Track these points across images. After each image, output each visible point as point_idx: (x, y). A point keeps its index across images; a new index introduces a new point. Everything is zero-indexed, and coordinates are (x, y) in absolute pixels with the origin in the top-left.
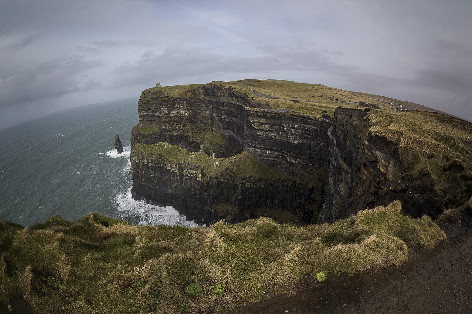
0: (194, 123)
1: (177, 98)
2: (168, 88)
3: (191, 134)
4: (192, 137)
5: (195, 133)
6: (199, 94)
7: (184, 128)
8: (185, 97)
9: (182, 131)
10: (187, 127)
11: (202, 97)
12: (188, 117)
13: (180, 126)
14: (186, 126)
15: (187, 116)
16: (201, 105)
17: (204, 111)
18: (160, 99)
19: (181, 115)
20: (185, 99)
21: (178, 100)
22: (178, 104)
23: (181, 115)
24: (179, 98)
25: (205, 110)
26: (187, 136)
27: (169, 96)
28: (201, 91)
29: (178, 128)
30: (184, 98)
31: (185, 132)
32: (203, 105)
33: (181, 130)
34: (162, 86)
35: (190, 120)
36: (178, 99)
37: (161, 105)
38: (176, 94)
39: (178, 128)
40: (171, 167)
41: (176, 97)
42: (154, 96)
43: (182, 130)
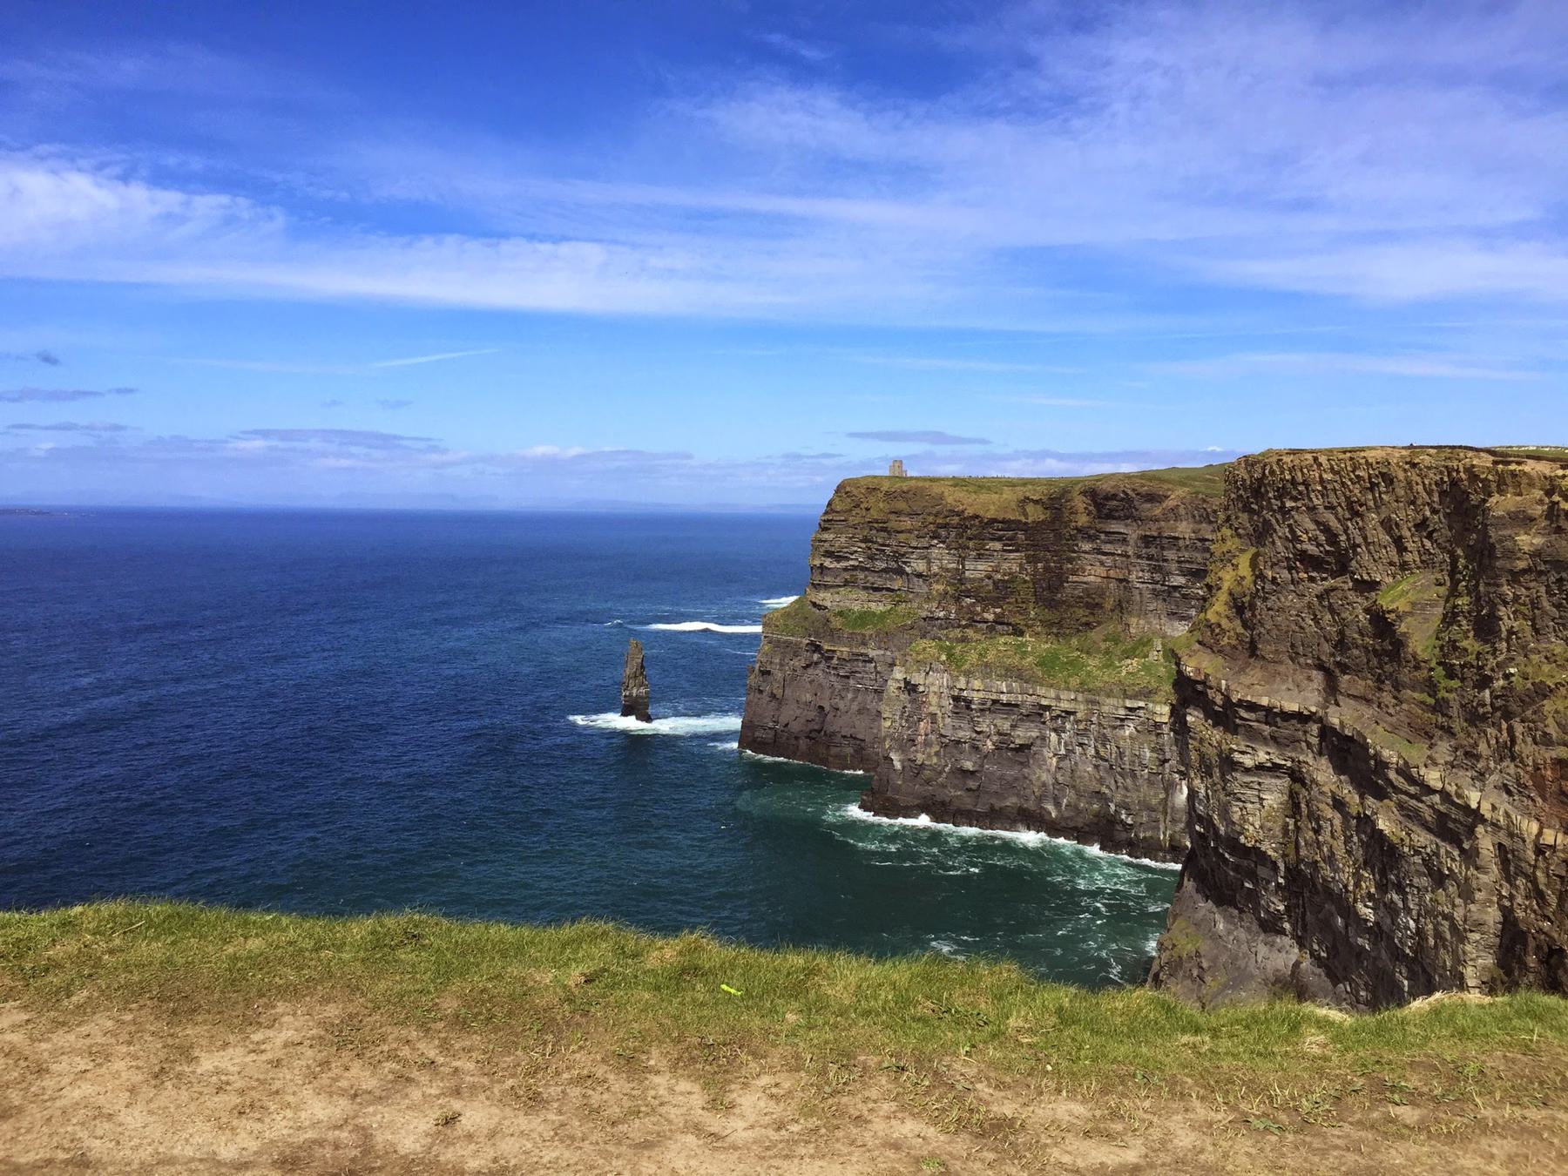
0: (1051, 604)
1: (994, 521)
5: (1057, 635)
11: (1083, 520)
14: (1024, 612)
18: (931, 519)
22: (999, 539)
28: (1080, 503)
29: (991, 617)
32: (1087, 546)
33: (1002, 623)
34: (909, 474)
37: (932, 538)
38: (989, 506)
40: (1058, 699)
41: (989, 515)
42: (901, 505)
43: (1008, 624)
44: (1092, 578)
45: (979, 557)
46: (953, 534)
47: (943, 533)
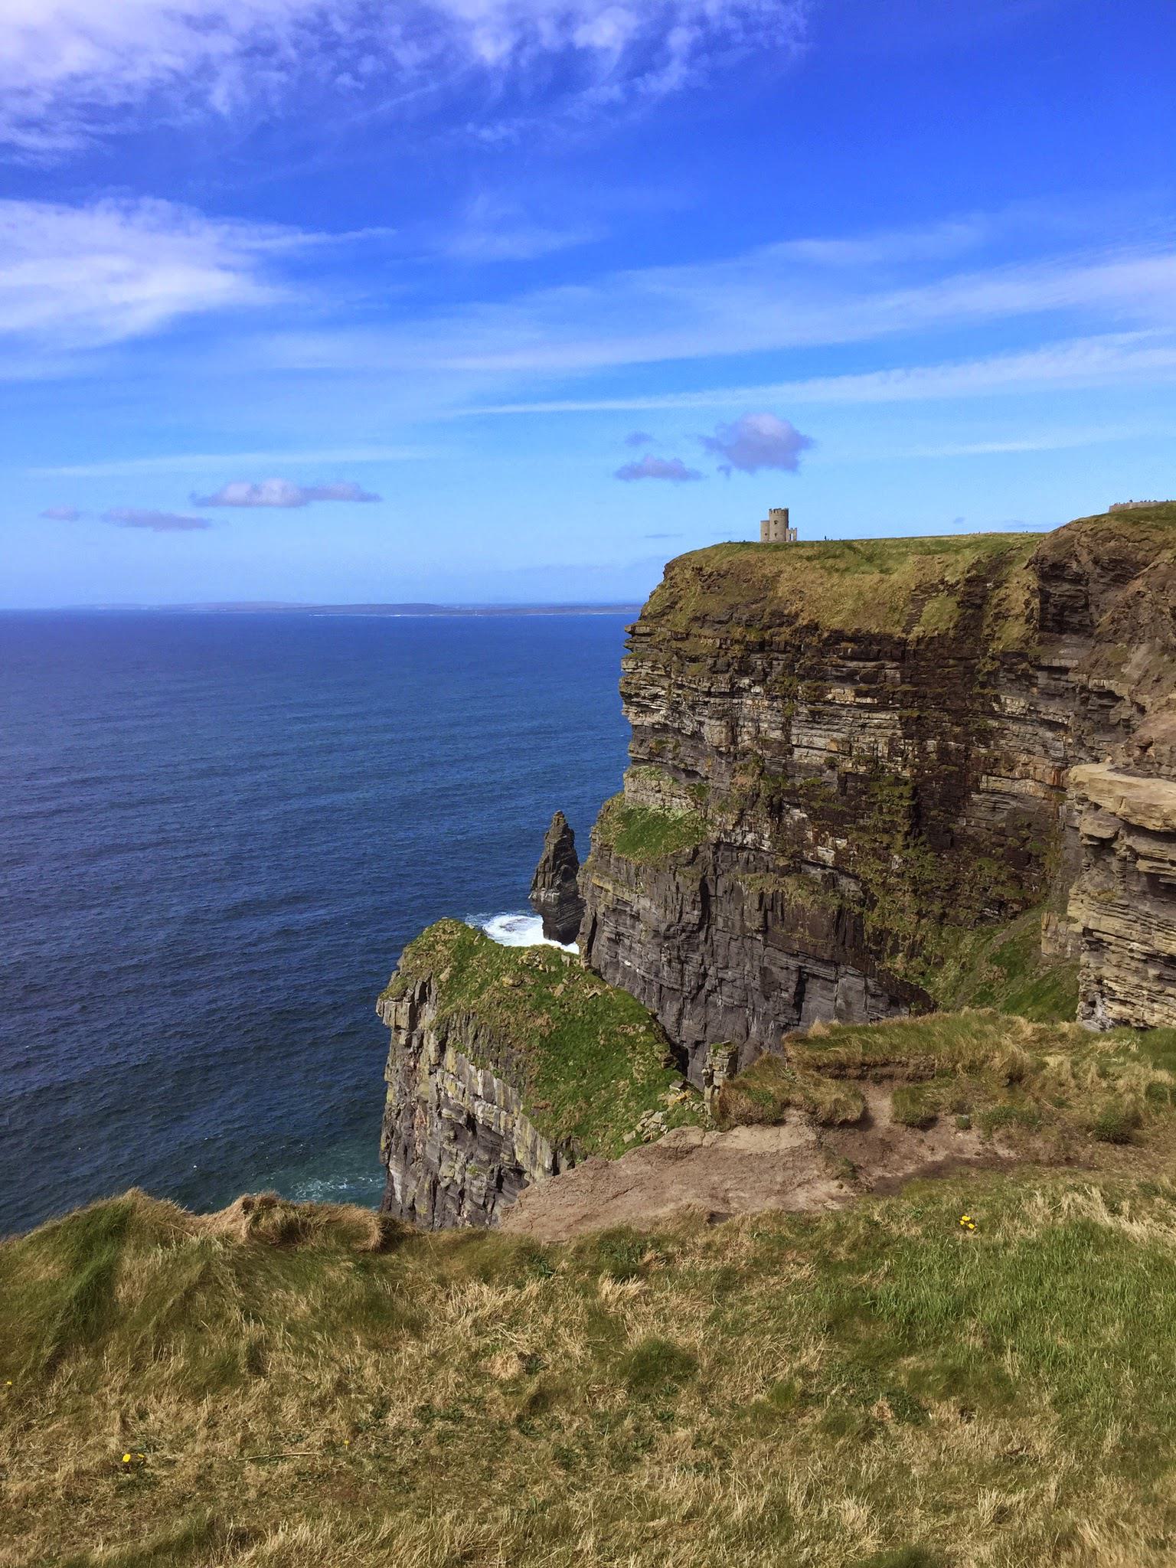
1: (838, 636)
2: (810, 552)
3: (904, 924)
4: (912, 954)
6: (997, 617)
7: (869, 870)
8: (897, 632)
9: (853, 887)
10: (886, 860)
12: (906, 791)
13: (842, 843)
14: (882, 855)
15: (898, 781)
16: (1003, 706)
17: (1024, 758)
19: (862, 769)
20: (900, 651)
21: (850, 647)
22: (848, 678)
23: (862, 769)
24: (854, 639)
25: (1029, 752)
26: (881, 936)
27: (797, 615)
28: (1019, 589)
29: (829, 856)
30: (891, 636)
31: (868, 901)
34: (801, 538)
35: (917, 814)
36: (850, 640)
38: (837, 603)
39: (829, 856)
41: (835, 622)
44: (1028, 787)
45: (815, 718)
46: (778, 667)
47: (758, 661)
